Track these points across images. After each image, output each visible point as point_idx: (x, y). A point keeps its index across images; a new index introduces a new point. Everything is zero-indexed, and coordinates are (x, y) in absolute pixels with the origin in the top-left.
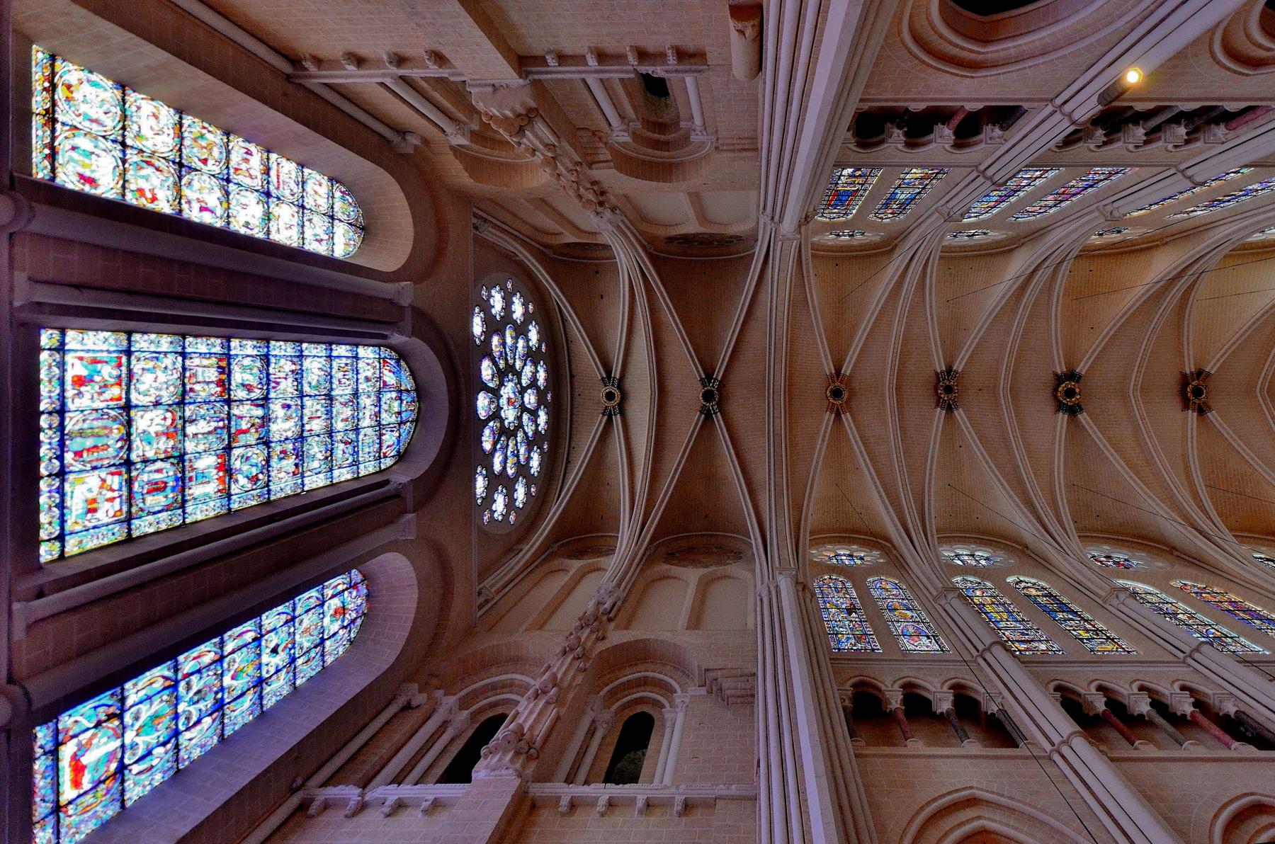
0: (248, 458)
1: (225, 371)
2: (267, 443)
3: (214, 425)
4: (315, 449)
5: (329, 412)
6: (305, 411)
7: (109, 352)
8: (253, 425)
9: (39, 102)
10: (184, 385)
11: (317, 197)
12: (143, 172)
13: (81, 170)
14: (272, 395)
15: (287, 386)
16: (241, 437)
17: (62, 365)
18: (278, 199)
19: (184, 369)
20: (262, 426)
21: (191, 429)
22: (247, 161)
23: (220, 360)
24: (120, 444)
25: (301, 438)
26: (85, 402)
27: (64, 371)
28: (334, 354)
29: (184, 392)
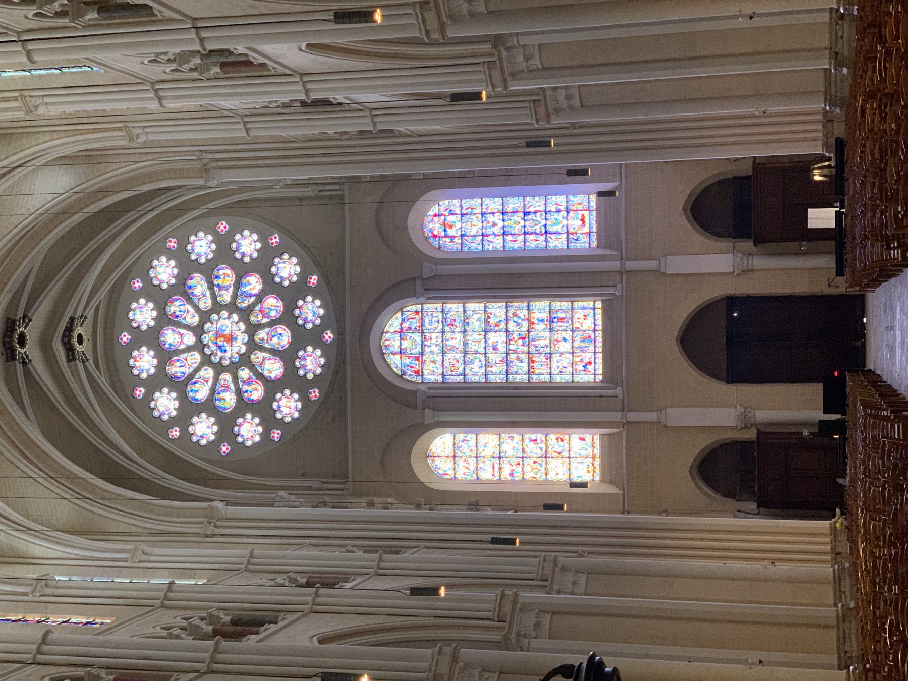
3: (536, 343)
4: (476, 323)
5: (465, 344)
9: (597, 462)
14: (505, 355)
15: (494, 357)
17: (595, 370)
21: (547, 342)
22: (513, 470)
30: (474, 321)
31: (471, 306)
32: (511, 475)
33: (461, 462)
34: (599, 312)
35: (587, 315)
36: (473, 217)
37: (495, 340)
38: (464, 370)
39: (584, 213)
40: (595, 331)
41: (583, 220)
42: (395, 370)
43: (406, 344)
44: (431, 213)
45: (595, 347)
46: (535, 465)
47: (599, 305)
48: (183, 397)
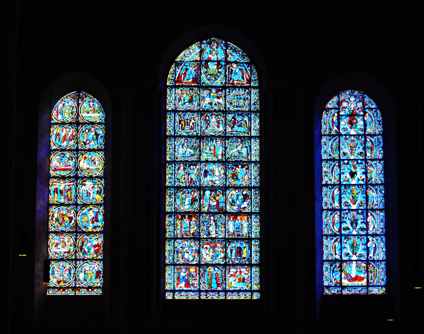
0: (233, 201)
1: (183, 214)
2: (225, 188)
3: (212, 222)
4: (236, 150)
5: (212, 138)
6: (210, 160)
7: (174, 273)
8: (215, 198)
9: (70, 293)
10: (190, 238)
11: (68, 137)
12: (86, 250)
13: (94, 278)
14: (198, 184)
15: (194, 172)
16: (221, 205)
17: (180, 291)
18: (77, 170)
19: (182, 238)
22: (61, 192)
24: (216, 269)
26: (196, 282)
27: (183, 290)
28: (173, 133)
30: (239, 148)
31: (255, 146)
32: (56, 191)
33: (70, 131)
34: (248, 296)
35: (242, 283)
36: (361, 150)
37: (217, 173)
38: (181, 136)
39: (365, 280)
40: (225, 291)
41: (357, 278)
42: (182, 55)
43: (212, 67)
44: (367, 99)
45: (206, 291)
46: (66, 219)
47: (256, 296)
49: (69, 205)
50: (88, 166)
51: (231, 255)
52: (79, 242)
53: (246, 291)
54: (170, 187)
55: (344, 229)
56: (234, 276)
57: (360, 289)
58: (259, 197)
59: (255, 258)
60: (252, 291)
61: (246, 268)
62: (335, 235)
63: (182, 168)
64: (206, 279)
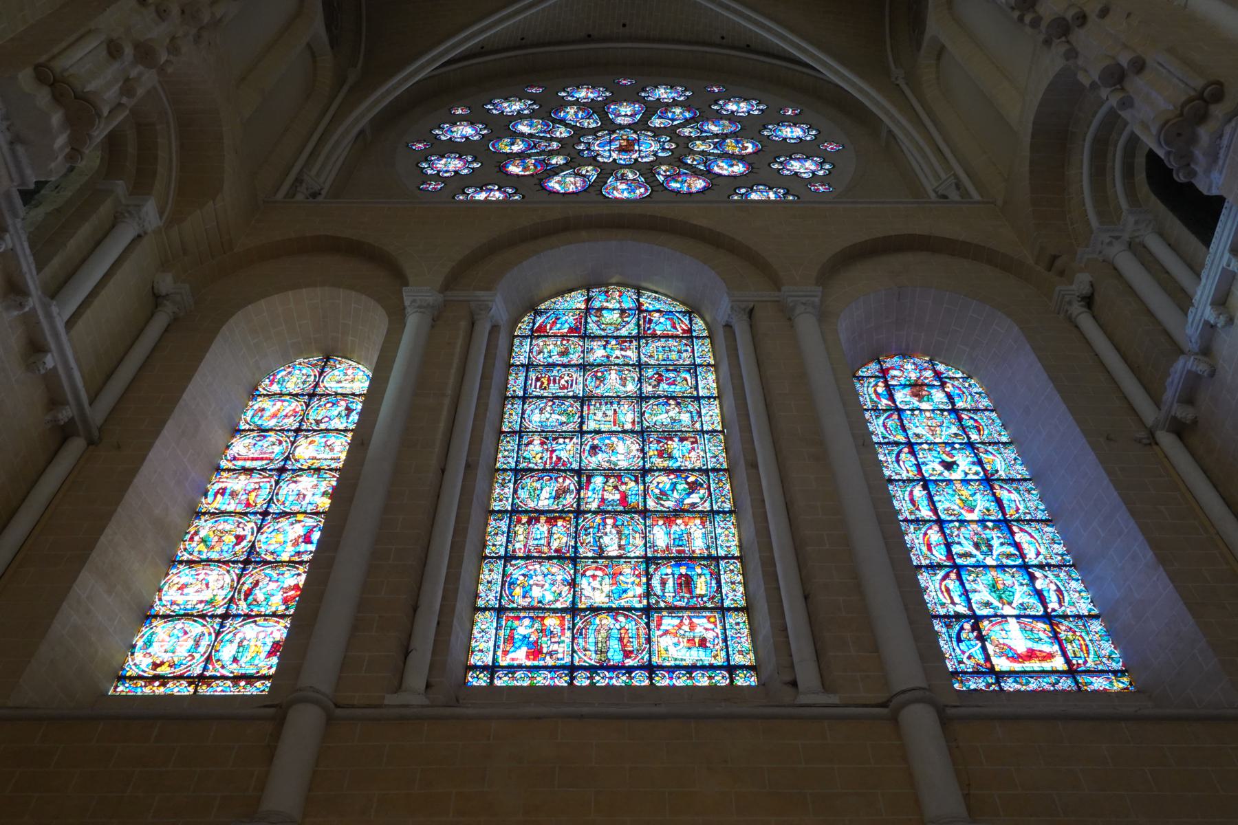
1: (535, 516)
8: (616, 488)
13: (264, 655)
14: (575, 466)
17: (512, 669)
19: (528, 558)
20: (619, 477)
23: (519, 521)
25: (642, 434)
27: (520, 667)
29: (559, 558)
40: (651, 669)
45: (591, 669)
46: (229, 539)
48: (520, 116)
49: (246, 514)
50: (315, 454)
51: (663, 590)
52: (248, 582)
53: (712, 667)
54: (505, 470)
55: (961, 556)
56: (675, 635)
57: (1053, 679)
58: (728, 486)
59: (734, 594)
60: (731, 669)
61: (708, 618)
62: (940, 566)
63: (537, 442)
64: (591, 640)
